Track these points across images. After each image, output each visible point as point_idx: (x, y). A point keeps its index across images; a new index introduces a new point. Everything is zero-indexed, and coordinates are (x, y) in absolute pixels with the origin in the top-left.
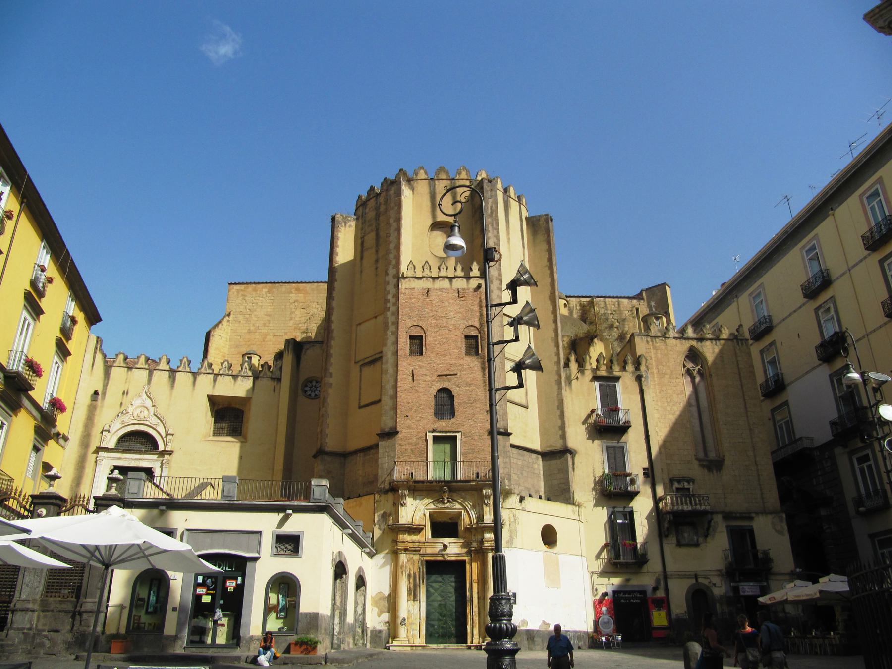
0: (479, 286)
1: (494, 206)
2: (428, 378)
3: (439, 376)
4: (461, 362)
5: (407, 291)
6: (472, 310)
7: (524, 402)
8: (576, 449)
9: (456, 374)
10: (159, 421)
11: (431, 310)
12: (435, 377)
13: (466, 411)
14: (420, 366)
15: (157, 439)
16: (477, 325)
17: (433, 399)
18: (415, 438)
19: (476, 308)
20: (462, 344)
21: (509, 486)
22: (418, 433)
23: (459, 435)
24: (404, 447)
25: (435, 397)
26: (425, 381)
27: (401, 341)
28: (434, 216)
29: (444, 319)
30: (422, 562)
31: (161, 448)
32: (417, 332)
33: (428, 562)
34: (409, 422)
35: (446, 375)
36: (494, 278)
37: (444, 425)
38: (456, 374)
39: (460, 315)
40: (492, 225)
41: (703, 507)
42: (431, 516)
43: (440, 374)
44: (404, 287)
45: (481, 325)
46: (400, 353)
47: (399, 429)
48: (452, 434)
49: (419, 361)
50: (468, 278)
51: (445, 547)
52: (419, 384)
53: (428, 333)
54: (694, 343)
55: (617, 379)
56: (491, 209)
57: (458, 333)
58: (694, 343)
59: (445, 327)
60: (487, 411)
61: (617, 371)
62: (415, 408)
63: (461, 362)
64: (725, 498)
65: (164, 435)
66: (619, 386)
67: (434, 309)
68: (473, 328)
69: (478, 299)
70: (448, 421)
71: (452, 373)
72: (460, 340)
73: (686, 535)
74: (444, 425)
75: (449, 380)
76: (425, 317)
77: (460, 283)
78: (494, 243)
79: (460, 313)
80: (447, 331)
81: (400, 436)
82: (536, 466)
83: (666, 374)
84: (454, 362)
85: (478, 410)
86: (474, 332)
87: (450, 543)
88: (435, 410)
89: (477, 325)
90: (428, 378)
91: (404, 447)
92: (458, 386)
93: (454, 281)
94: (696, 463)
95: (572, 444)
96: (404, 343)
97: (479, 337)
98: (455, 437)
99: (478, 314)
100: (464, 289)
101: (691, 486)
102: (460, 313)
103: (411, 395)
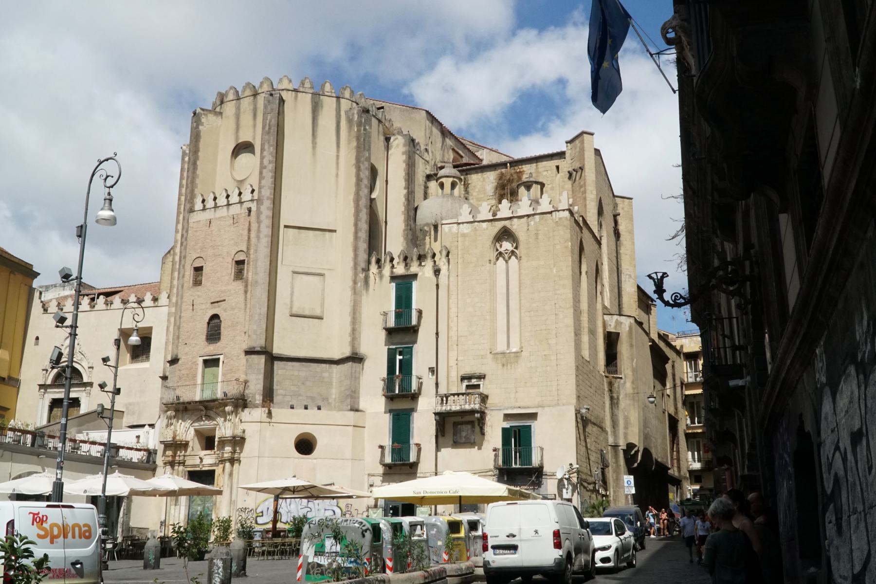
0: (250, 210)
1: (273, 120)
2: (203, 307)
3: (212, 303)
4: (229, 287)
5: (195, 224)
6: (242, 235)
7: (318, 312)
8: (367, 354)
9: (225, 300)
10: (83, 356)
11: (211, 240)
12: (209, 304)
13: (229, 334)
14: (199, 296)
15: (82, 372)
16: (245, 250)
17: (206, 325)
18: (190, 363)
19: (246, 232)
20: (231, 269)
21: (259, 400)
22: (193, 358)
23: (221, 357)
24: (183, 372)
25: (209, 323)
26: (201, 309)
27: (187, 273)
28: (237, 138)
29: (220, 248)
30: (185, 472)
31: (85, 380)
32: (198, 264)
33: (189, 472)
34: (187, 349)
35: (217, 302)
36: (265, 198)
37: (211, 349)
38: (225, 300)
39: (233, 241)
40: (269, 143)
41: (472, 406)
42: (196, 431)
43: (213, 301)
44: (193, 221)
45: (248, 249)
46: (186, 285)
47: (179, 356)
48: (214, 357)
49: (198, 291)
50: (241, 203)
51: (201, 459)
52: (197, 312)
53: (207, 263)
54: (507, 223)
55: (415, 276)
56: (269, 125)
57: (230, 260)
58: (507, 223)
59: (220, 255)
60: (245, 333)
61: (414, 269)
62: (192, 335)
63: (229, 287)
64: (517, 392)
65: (86, 367)
66: (415, 285)
67: (213, 239)
68: (242, 253)
69: (248, 223)
70: (215, 345)
71: (222, 299)
72: (230, 266)
73: (464, 434)
74: (211, 349)
75: (219, 307)
76: (206, 248)
77: (235, 210)
78: (269, 161)
79: (233, 239)
80: (221, 259)
81: (180, 362)
82: (326, 375)
83: (471, 263)
84: (224, 288)
85: (238, 332)
86: (241, 257)
87: (205, 455)
88: (207, 336)
89: (245, 250)
90: (203, 307)
91: (183, 372)
92: (225, 310)
93: (231, 207)
94: (490, 356)
95: (363, 350)
96: (189, 273)
97: (246, 261)
98: (219, 359)
99: (246, 238)
100: (238, 214)
101: (481, 383)
102: (233, 239)
103: (191, 324)
